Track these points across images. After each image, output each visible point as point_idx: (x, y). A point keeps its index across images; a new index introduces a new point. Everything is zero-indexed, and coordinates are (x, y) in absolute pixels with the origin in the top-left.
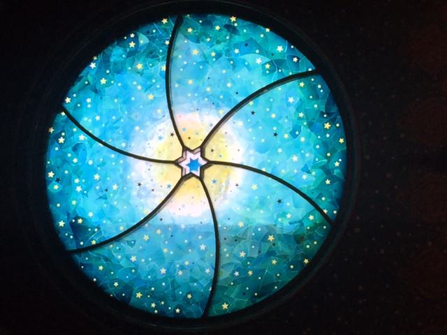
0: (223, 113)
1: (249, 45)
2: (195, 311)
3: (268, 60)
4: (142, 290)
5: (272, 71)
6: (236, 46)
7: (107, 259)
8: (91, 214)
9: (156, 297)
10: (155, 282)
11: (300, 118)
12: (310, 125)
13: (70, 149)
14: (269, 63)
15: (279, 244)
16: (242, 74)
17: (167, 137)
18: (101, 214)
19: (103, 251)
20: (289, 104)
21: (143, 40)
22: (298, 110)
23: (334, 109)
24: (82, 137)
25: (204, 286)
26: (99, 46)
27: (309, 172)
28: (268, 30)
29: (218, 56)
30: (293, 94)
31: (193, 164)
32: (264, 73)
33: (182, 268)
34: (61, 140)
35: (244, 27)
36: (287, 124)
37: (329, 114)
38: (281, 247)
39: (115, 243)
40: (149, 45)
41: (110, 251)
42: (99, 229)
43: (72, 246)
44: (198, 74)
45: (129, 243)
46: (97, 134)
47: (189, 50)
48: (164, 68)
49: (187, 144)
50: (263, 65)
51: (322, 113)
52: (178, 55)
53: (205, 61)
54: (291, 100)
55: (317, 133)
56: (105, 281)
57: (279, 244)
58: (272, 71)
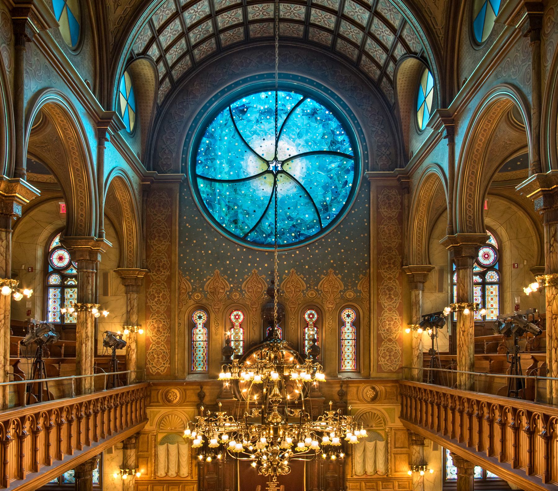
0: (300, 181)
1: (336, 194)
3: (328, 203)
4: (210, 143)
5: (323, 206)
6: (336, 187)
7: (225, 124)
8: (249, 115)
10: (214, 150)
11: (297, 220)
12: (294, 226)
13: (283, 103)
14: (327, 204)
15: (233, 211)
16: (320, 191)
17: (288, 152)
18: (249, 121)
19: (230, 122)
20: (304, 215)
22: (302, 220)
23: (302, 238)
27: (269, 226)
28: (344, 203)
29: (331, 178)
32: (320, 202)
33: (221, 163)
34: (288, 98)
35: (346, 190)
36: (294, 215)
37: (299, 235)
39: (234, 128)
40: (338, 142)
41: (230, 126)
42: (241, 120)
44: (321, 168)
45: (234, 135)
48: (325, 150)
49: (285, 164)
50: (325, 201)
51: (299, 232)
54: (307, 216)
55: (290, 229)
56: (214, 124)
57: (233, 211)
58: (323, 206)
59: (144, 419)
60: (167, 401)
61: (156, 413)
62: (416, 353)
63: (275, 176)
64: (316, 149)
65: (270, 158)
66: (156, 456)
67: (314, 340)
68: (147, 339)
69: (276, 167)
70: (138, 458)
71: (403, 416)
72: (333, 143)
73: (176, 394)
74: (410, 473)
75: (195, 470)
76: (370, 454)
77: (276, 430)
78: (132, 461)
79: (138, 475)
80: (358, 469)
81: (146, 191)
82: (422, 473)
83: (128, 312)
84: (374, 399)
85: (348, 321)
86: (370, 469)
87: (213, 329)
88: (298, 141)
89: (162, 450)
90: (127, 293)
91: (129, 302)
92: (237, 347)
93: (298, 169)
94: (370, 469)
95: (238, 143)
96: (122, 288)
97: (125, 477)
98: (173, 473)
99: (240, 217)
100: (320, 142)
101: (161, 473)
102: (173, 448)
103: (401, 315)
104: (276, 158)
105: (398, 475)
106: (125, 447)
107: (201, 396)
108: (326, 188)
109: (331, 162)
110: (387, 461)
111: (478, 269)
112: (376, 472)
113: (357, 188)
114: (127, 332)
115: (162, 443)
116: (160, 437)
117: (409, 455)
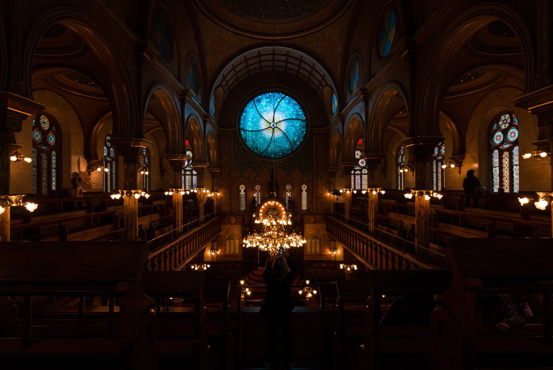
1: (299, 137)
2: (241, 126)
9: (244, 118)
10: (247, 118)
18: (262, 106)
21: (300, 113)
24: (279, 100)
25: (247, 128)
26: (299, 103)
30: (287, 146)
31: (274, 125)
36: (281, 145)
38: (255, 145)
43: (255, 99)
44: (292, 126)
46: (280, 104)
47: (298, 124)
52: (297, 121)
53: (295, 127)
56: (248, 107)
59: (220, 230)
60: (230, 223)
61: (225, 227)
62: (332, 203)
63: (273, 129)
64: (290, 117)
65: (271, 121)
66: (225, 245)
67: (290, 198)
68: (221, 197)
69: (274, 125)
70: (217, 246)
71: (327, 229)
72: (298, 115)
73: (233, 220)
74: (330, 253)
75: (241, 251)
76: (313, 245)
77: (275, 241)
78: (215, 247)
79: (218, 253)
80: (308, 250)
81: (219, 137)
82: (335, 253)
83: (213, 186)
84: (315, 222)
85: (304, 189)
86: (313, 251)
87: (248, 193)
88: (283, 114)
89: (227, 243)
90: (212, 178)
91: (213, 182)
92: (258, 200)
93: (283, 126)
94: (313, 251)
95: (258, 116)
96: (210, 176)
97: (213, 253)
98: (232, 252)
99: (259, 146)
100: (292, 115)
101: (228, 252)
102: (232, 242)
103: (326, 187)
104: (274, 121)
105: (326, 253)
106: (213, 242)
107: (243, 220)
108: (294, 134)
109: (297, 123)
110: (320, 248)
111: (359, 168)
112: (316, 252)
113: (308, 134)
114: (213, 194)
115: (227, 240)
116: (227, 237)
117: (330, 246)
